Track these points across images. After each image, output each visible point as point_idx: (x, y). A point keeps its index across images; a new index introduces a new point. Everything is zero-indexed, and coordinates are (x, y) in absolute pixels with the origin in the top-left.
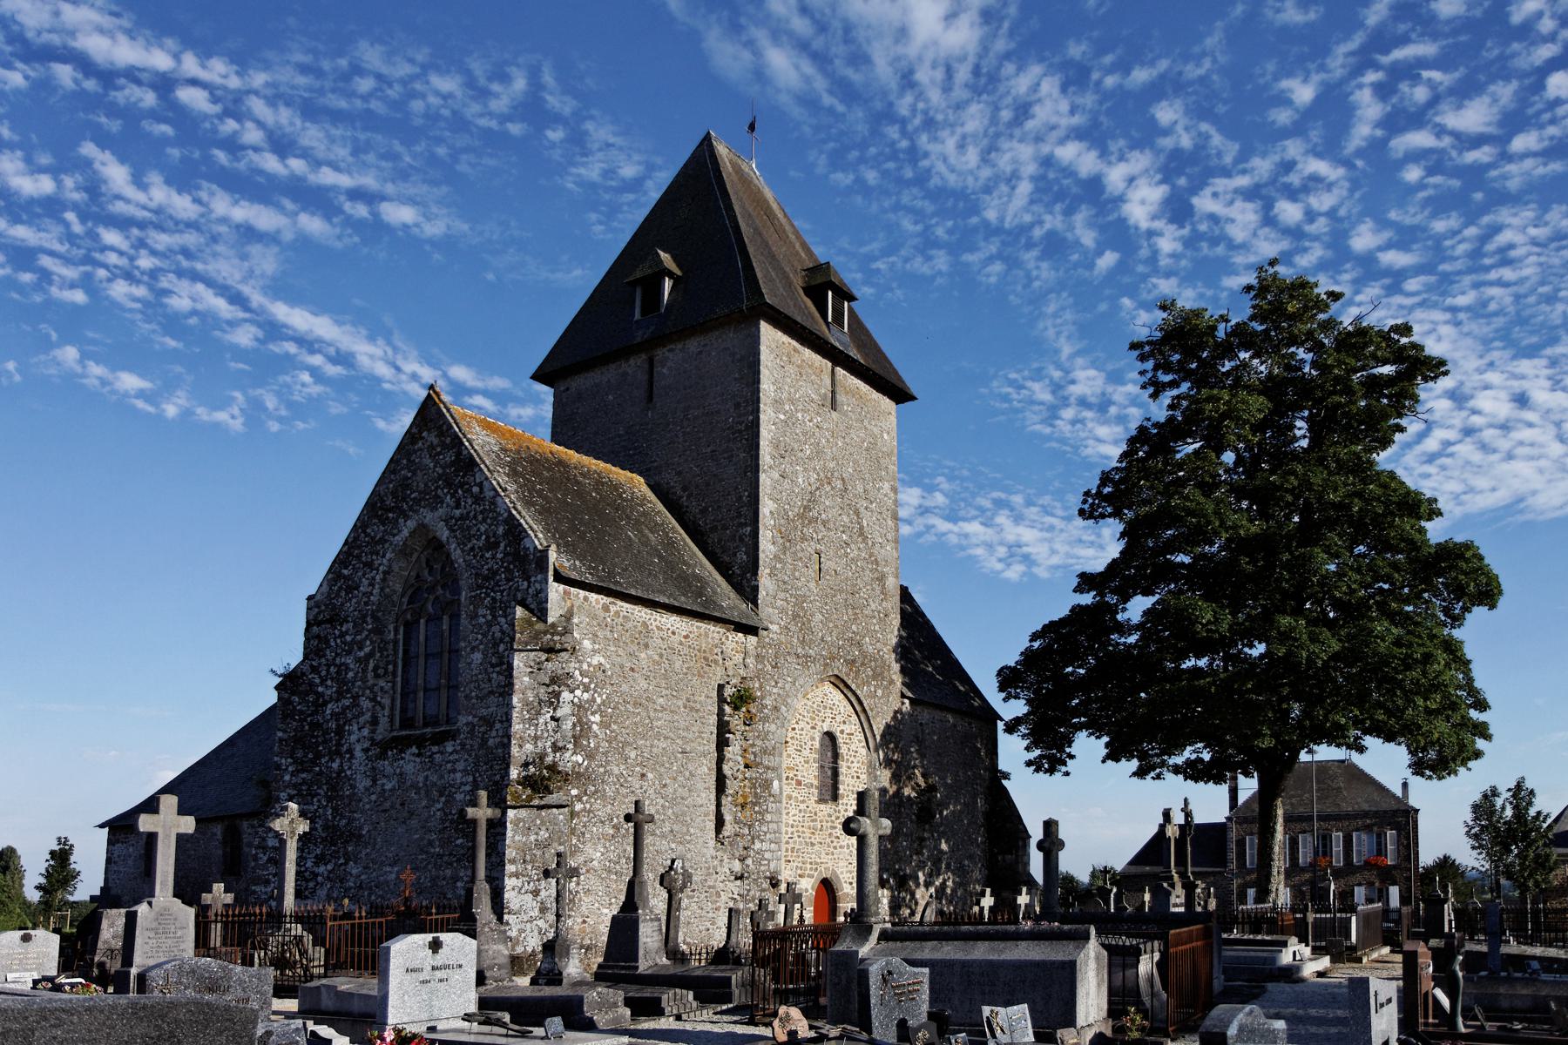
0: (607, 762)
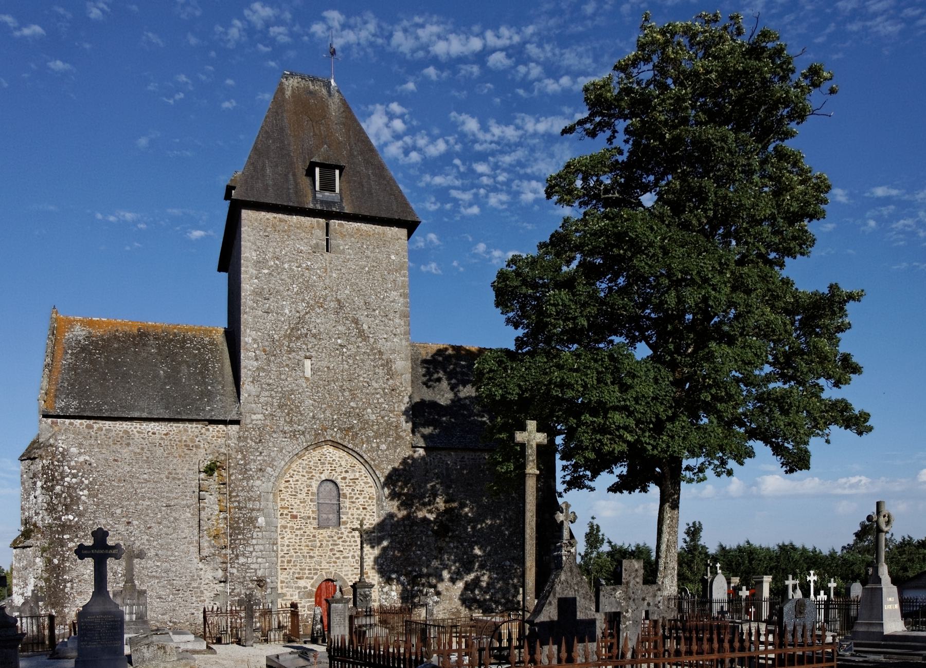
0: (96, 518)
